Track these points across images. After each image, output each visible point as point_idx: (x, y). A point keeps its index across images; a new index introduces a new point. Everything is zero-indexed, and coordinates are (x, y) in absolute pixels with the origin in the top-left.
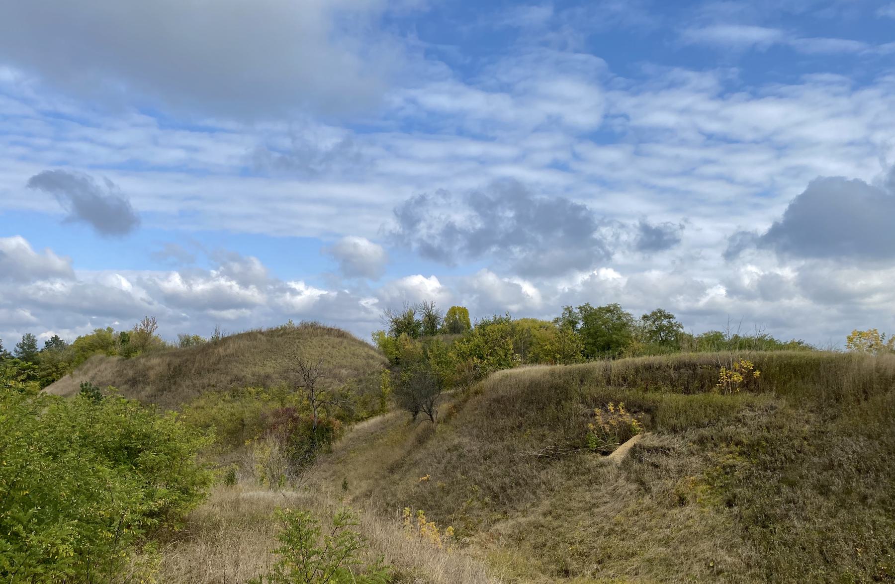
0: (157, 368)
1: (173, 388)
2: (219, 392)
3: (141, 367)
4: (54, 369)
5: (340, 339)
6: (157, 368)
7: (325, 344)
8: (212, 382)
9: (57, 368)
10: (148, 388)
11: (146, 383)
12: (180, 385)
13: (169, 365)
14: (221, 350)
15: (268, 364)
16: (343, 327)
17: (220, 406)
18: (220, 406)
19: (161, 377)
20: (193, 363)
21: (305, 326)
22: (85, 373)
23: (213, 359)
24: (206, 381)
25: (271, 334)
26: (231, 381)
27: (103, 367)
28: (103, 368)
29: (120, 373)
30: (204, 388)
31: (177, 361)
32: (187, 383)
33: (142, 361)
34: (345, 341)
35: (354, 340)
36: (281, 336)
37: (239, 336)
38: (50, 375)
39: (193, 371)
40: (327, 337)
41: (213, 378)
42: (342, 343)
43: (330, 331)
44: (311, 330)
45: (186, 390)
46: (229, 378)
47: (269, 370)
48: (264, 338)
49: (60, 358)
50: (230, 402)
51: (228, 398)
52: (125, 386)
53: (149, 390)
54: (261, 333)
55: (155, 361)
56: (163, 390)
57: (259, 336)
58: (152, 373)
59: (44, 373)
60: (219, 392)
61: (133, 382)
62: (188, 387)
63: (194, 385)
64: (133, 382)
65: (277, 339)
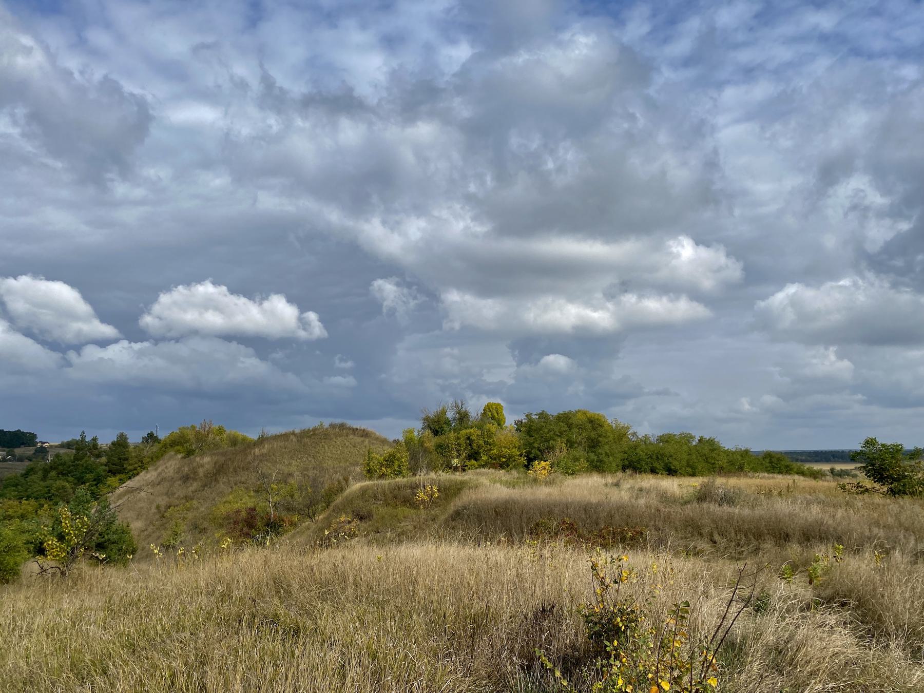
0: (207, 466)
1: (213, 483)
2: (247, 488)
3: (195, 464)
4: (140, 464)
5: (362, 439)
6: (207, 466)
7: (347, 444)
8: (243, 479)
9: (142, 462)
10: (195, 484)
11: (195, 480)
13: (215, 463)
14: (257, 451)
15: (294, 462)
17: (244, 501)
18: (244, 501)
20: (233, 462)
24: (238, 478)
27: (169, 464)
28: (171, 464)
29: (179, 470)
30: (236, 484)
31: (222, 459)
35: (377, 439)
36: (310, 437)
40: (351, 437)
42: (363, 442)
45: (222, 486)
47: (293, 469)
51: (252, 493)
52: (179, 482)
53: (195, 485)
54: (293, 433)
55: (207, 459)
56: (205, 486)
57: (292, 437)
58: (201, 472)
61: (186, 479)
64: (186, 479)
65: (306, 440)
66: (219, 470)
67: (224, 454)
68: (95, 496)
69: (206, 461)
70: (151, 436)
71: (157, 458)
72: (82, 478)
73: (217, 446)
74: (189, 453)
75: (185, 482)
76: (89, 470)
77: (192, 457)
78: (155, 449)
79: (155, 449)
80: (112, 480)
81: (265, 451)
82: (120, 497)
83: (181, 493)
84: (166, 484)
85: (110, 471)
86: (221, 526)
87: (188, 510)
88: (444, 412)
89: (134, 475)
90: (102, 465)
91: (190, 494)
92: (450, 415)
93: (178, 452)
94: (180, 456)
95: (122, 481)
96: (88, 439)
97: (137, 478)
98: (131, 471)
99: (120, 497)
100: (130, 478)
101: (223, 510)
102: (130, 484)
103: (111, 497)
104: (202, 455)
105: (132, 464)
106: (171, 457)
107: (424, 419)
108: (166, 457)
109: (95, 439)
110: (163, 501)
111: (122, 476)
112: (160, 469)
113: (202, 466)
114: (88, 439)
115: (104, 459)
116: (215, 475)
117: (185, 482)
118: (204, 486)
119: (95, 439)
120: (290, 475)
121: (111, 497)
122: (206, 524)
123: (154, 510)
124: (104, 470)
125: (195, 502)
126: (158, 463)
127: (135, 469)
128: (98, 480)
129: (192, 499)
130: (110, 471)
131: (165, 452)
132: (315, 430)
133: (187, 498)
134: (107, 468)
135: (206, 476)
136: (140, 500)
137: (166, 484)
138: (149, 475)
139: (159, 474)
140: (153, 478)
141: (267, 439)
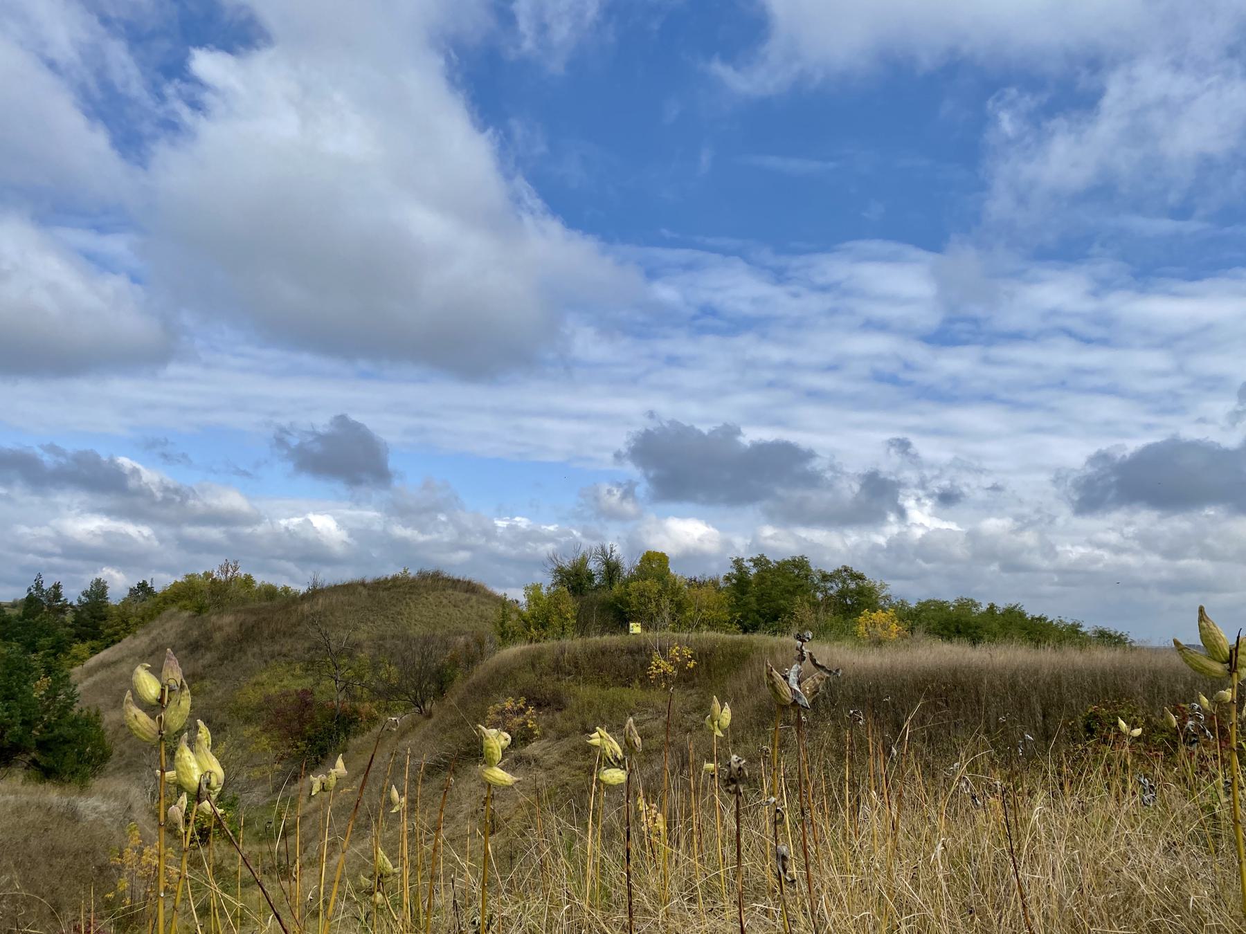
2: (290, 664)
3: (209, 626)
4: (124, 625)
5: (468, 595)
7: (445, 601)
8: (285, 650)
9: (127, 624)
10: (208, 656)
11: (208, 649)
12: (245, 653)
14: (306, 607)
15: (363, 627)
16: (475, 577)
18: (285, 682)
19: (228, 641)
21: (423, 576)
22: (148, 634)
23: (294, 620)
24: (277, 648)
26: (309, 649)
27: (168, 626)
28: (172, 625)
29: (184, 635)
30: (273, 657)
31: (251, 619)
32: (256, 649)
33: (214, 618)
34: (474, 598)
37: (335, 589)
38: (116, 633)
39: (266, 634)
40: (450, 591)
41: (286, 645)
42: (468, 600)
43: (455, 584)
44: (429, 581)
46: (307, 645)
47: (361, 636)
48: (365, 592)
49: (133, 611)
50: (300, 678)
51: (298, 672)
52: (184, 652)
53: (209, 657)
54: (363, 584)
55: (228, 619)
57: (361, 588)
58: (218, 637)
59: (110, 631)
60: (290, 664)
62: (254, 655)
63: (262, 654)
65: (382, 594)
66: (247, 635)
67: (252, 612)
68: (49, 671)
69: (227, 621)
70: (143, 586)
71: (152, 618)
72: (33, 644)
73: (244, 601)
74: (200, 610)
75: (192, 652)
77: (205, 615)
78: (147, 604)
79: (147, 604)
80: (79, 648)
81: (319, 608)
85: (77, 635)
86: (248, 721)
88: (584, 561)
89: (113, 642)
90: (66, 625)
91: (200, 670)
92: (593, 566)
93: (184, 608)
94: (186, 614)
95: (94, 651)
96: (47, 586)
97: (118, 646)
98: (109, 636)
100: (107, 647)
101: (252, 696)
102: (104, 655)
103: (77, 671)
104: (220, 614)
105: (111, 627)
106: (172, 616)
107: (556, 571)
108: (165, 614)
109: (57, 587)
111: (96, 643)
112: (154, 633)
113: (220, 628)
114: (47, 586)
115: (69, 618)
116: (240, 641)
117: (192, 652)
118: (222, 659)
119: (57, 587)
120: (358, 645)
121: (77, 671)
122: (223, 717)
124: (68, 634)
125: (207, 684)
126: (152, 624)
127: (116, 633)
128: (60, 648)
129: (203, 678)
130: (77, 635)
131: (163, 609)
132: (395, 579)
134: (73, 631)
136: (120, 679)
138: (137, 642)
139: (154, 640)
140: (143, 645)
141: (322, 590)
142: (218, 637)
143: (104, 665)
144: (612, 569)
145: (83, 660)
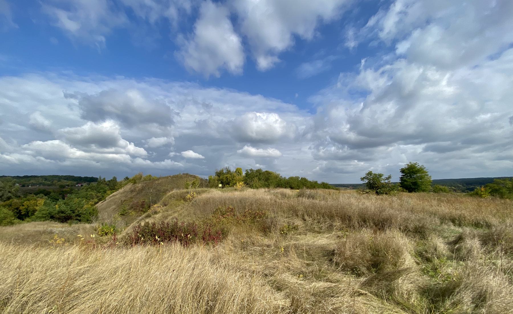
25: (174, 177)
37: (164, 178)
43: (191, 176)
53: (134, 193)
55: (140, 185)
61: (132, 191)
69: (139, 185)
74: (135, 183)
76: (102, 188)
80: (108, 192)
82: (110, 197)
83: (129, 196)
84: (126, 193)
87: (131, 202)
88: (223, 170)
92: (224, 172)
96: (102, 178)
99: (110, 197)
109: (104, 179)
110: (123, 199)
114: (102, 178)
119: (104, 179)
123: (120, 202)
133: (131, 198)
135: (139, 190)
137: (126, 193)
142: (137, 189)
143: (113, 196)
144: (229, 172)
145: (109, 195)
